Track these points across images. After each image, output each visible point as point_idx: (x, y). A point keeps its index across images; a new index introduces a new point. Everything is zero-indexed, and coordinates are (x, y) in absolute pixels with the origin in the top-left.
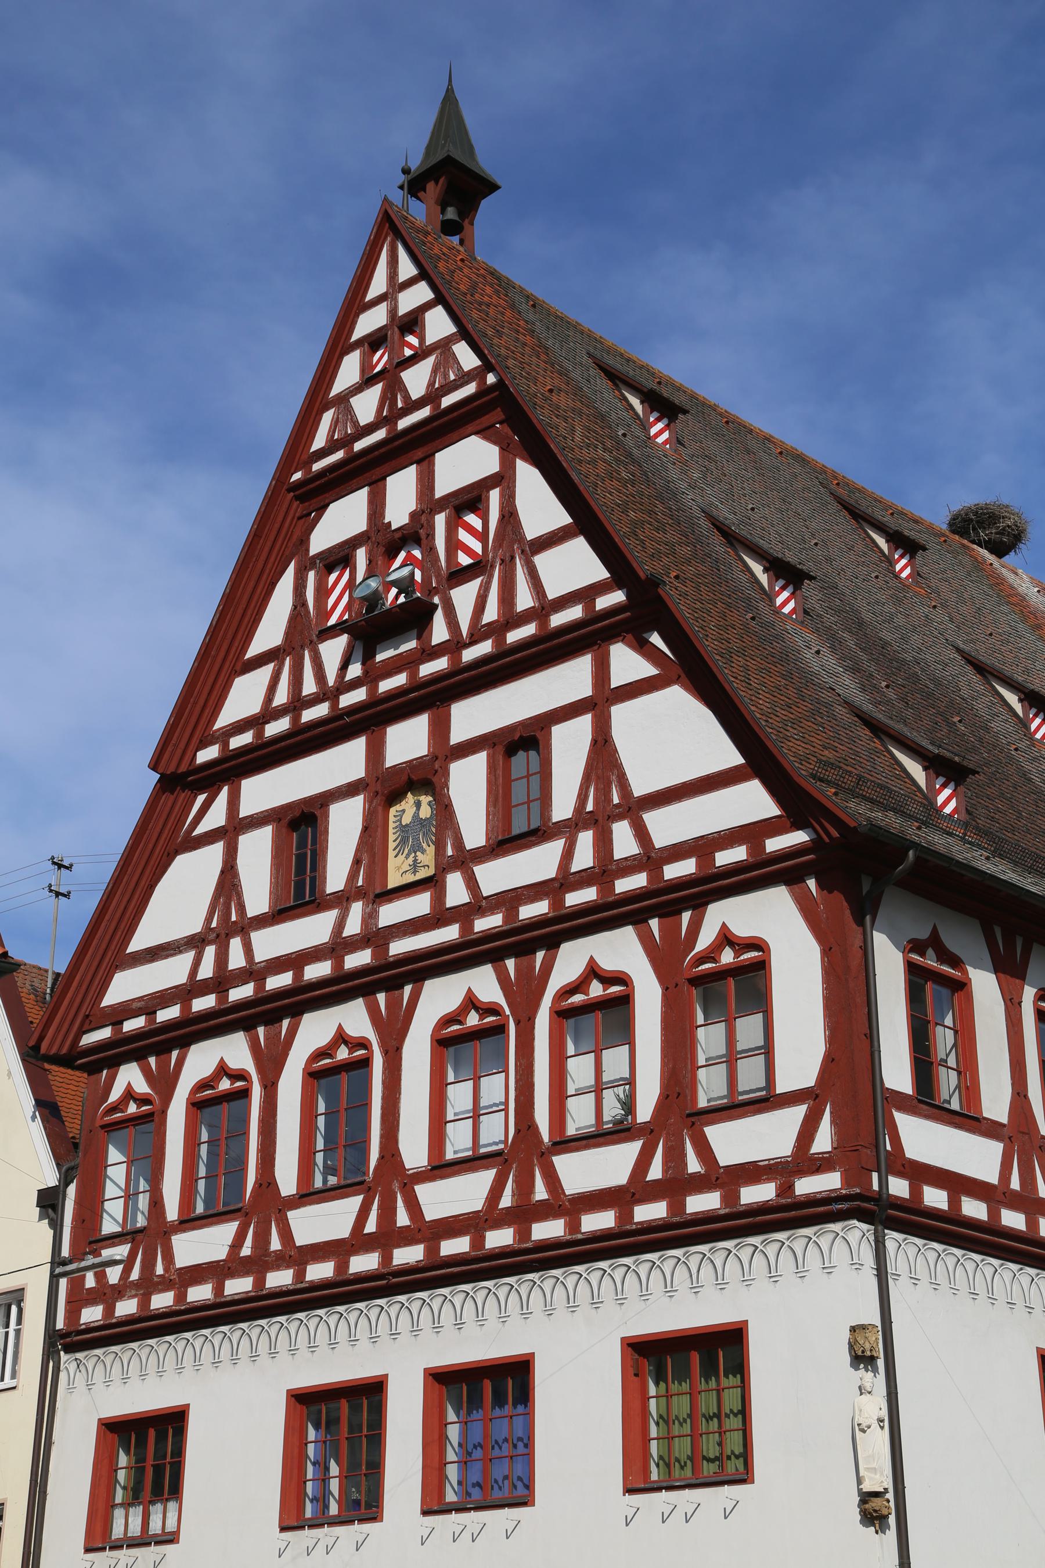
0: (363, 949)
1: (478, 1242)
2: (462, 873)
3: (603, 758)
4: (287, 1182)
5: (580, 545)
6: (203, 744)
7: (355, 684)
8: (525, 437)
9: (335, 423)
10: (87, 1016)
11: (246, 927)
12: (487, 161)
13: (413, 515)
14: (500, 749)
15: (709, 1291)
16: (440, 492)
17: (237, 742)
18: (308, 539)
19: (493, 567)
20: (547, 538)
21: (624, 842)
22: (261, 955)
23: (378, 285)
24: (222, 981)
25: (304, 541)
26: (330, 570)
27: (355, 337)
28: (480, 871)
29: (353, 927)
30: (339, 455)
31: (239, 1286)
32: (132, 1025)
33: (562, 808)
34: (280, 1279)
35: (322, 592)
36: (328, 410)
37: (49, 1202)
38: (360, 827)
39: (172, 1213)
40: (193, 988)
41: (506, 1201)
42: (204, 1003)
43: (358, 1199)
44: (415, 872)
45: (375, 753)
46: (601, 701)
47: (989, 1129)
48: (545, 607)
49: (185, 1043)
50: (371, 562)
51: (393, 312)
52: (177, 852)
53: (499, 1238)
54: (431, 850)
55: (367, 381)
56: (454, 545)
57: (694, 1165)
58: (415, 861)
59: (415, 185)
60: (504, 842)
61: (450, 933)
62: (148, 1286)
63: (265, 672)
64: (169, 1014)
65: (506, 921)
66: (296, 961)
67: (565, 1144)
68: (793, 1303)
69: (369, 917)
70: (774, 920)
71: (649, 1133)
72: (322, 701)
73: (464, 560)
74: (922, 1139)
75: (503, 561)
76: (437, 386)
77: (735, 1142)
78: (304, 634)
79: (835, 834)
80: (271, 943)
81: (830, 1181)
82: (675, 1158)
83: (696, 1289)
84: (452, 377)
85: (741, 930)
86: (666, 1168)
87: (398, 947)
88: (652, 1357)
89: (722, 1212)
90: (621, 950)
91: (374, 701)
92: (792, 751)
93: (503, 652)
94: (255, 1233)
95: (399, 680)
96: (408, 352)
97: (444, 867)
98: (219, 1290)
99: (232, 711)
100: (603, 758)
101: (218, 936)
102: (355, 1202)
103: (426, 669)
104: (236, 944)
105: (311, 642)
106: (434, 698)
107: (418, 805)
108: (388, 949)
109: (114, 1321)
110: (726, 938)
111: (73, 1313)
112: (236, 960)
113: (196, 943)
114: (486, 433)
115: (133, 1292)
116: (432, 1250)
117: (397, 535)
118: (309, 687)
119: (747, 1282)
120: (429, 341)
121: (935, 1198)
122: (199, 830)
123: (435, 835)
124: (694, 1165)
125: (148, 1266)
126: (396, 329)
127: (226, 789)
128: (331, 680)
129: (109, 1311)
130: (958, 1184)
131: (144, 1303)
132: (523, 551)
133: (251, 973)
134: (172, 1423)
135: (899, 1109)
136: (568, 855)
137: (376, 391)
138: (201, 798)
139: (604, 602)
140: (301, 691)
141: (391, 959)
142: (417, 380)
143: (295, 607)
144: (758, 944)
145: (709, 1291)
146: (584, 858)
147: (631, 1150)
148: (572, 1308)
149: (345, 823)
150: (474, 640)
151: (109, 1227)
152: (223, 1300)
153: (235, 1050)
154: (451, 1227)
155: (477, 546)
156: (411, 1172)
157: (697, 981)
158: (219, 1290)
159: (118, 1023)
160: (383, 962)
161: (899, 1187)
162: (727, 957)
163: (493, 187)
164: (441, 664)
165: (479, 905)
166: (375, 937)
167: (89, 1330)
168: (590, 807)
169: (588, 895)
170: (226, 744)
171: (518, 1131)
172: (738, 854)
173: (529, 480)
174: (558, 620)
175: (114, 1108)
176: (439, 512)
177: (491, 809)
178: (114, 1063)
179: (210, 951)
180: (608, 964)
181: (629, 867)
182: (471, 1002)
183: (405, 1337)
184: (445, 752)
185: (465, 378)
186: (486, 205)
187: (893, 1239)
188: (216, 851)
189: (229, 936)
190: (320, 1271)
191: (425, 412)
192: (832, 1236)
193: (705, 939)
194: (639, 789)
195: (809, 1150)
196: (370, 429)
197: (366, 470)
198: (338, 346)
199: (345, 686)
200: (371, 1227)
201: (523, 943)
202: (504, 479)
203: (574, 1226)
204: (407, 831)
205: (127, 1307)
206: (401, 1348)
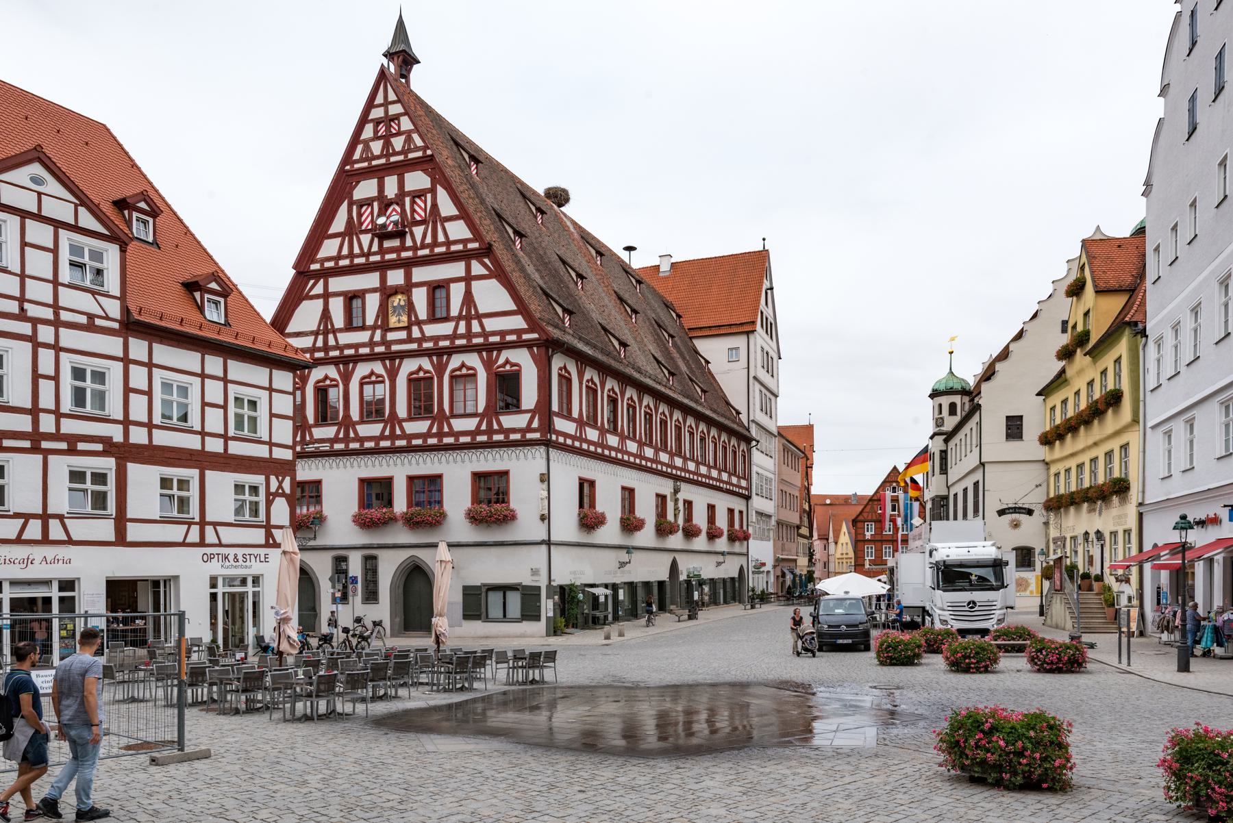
3: (468, 299)
6: (313, 262)
7: (375, 254)
11: (335, 331)
15: (498, 461)
16: (407, 189)
21: (476, 327)
23: (380, 99)
26: (362, 206)
29: (377, 338)
30: (366, 164)
33: (454, 312)
35: (360, 215)
41: (434, 430)
43: (382, 425)
45: (383, 279)
46: (468, 279)
48: (448, 243)
50: (380, 209)
53: (432, 441)
55: (376, 137)
56: (413, 211)
57: (496, 427)
60: (433, 319)
61: (414, 346)
66: (356, 346)
68: (524, 468)
69: (383, 336)
70: (523, 360)
71: (482, 416)
73: (418, 218)
74: (561, 424)
77: (508, 421)
78: (352, 230)
81: (537, 435)
82: (490, 424)
85: (512, 360)
87: (394, 348)
90: (473, 360)
91: (383, 261)
95: (394, 256)
100: (468, 299)
103: (404, 254)
104: (331, 337)
106: (408, 265)
110: (507, 362)
112: (332, 342)
113: (316, 334)
114: (425, 171)
119: (510, 459)
120: (402, 129)
121: (561, 440)
124: (496, 427)
130: (566, 435)
136: (456, 328)
138: (312, 282)
139: (470, 246)
142: (398, 143)
145: (498, 461)
147: (477, 420)
166: (384, 342)
169: (463, 342)
172: (513, 338)
173: (442, 193)
174: (453, 248)
179: (321, 338)
180: (469, 363)
181: (477, 335)
182: (420, 369)
185: (417, 149)
188: (319, 303)
193: (501, 361)
194: (481, 311)
196: (378, 157)
197: (379, 173)
198: (363, 120)
201: (440, 354)
202: (433, 191)
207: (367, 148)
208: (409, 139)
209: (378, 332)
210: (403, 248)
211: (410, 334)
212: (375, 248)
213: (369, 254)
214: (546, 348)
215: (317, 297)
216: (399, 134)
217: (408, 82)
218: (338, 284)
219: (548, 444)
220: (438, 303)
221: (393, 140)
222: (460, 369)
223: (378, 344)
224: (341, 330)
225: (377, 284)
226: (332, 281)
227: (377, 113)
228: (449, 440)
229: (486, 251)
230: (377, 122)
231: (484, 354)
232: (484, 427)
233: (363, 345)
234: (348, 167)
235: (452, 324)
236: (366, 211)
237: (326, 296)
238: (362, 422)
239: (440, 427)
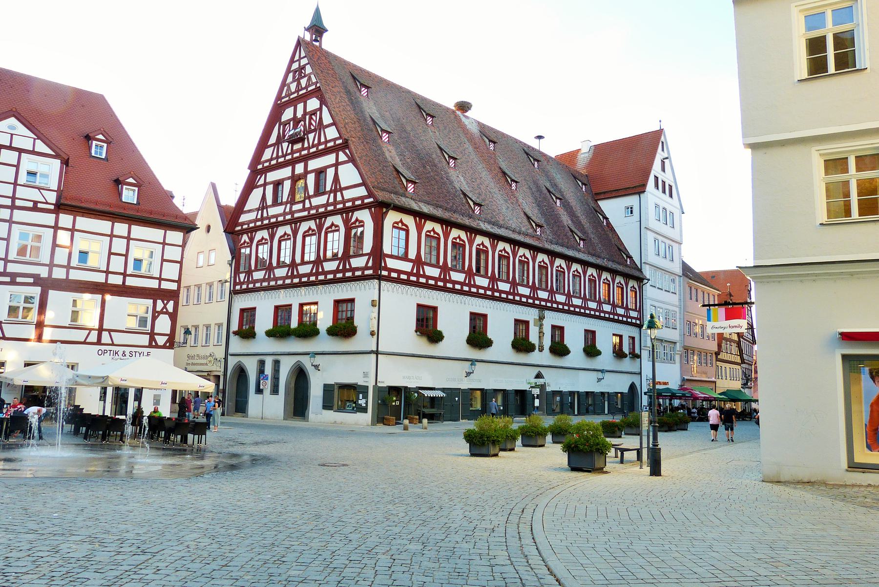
8: (323, 102)
11: (267, 207)
12: (326, 23)
17: (266, 164)
22: (270, 214)
24: (262, 219)
28: (312, 200)
29: (288, 210)
31: (265, 284)
32: (245, 227)
33: (328, 189)
34: (273, 283)
35: (284, 131)
39: (253, 268)
40: (256, 220)
42: (259, 223)
46: (337, 164)
47: (410, 261)
48: (327, 142)
49: (256, 231)
55: (294, 81)
56: (310, 124)
57: (348, 267)
59: (307, 29)
61: (306, 213)
62: (248, 282)
64: (252, 225)
66: (276, 216)
67: (326, 260)
68: (362, 294)
69: (291, 208)
73: (312, 128)
80: (273, 211)
81: (370, 272)
85: (360, 219)
87: (296, 215)
88: (337, 302)
90: (338, 220)
91: (293, 158)
93: (318, 151)
106: (305, 159)
110: (357, 220)
111: (234, 287)
112: (265, 215)
113: (258, 209)
116: (300, 280)
118: (280, 154)
121: (394, 275)
124: (348, 267)
130: (400, 272)
142: (303, 82)
144: (362, 221)
146: (331, 200)
154: (304, 275)
161: (385, 273)
162: (357, 224)
164: (305, 152)
165: (311, 208)
166: (292, 212)
169: (331, 208)
174: (329, 145)
180: (335, 223)
181: (340, 203)
182: (310, 229)
184: (306, 172)
186: (325, 35)
187: (383, 283)
190: (280, 282)
193: (353, 220)
196: (294, 93)
198: (288, 71)
201: (320, 217)
203: (326, 277)
205: (244, 287)
208: (309, 79)
209: (289, 205)
210: (303, 149)
211: (304, 205)
212: (289, 151)
213: (287, 155)
214: (380, 208)
215: (261, 186)
216: (305, 76)
217: (321, 44)
218: (272, 176)
219: (380, 278)
221: (301, 81)
222: (330, 227)
223: (287, 214)
224: (270, 206)
225: (290, 174)
229: (345, 146)
230: (295, 71)
232: (341, 268)
233: (280, 215)
235: (327, 196)
237: (265, 185)
239: (317, 269)
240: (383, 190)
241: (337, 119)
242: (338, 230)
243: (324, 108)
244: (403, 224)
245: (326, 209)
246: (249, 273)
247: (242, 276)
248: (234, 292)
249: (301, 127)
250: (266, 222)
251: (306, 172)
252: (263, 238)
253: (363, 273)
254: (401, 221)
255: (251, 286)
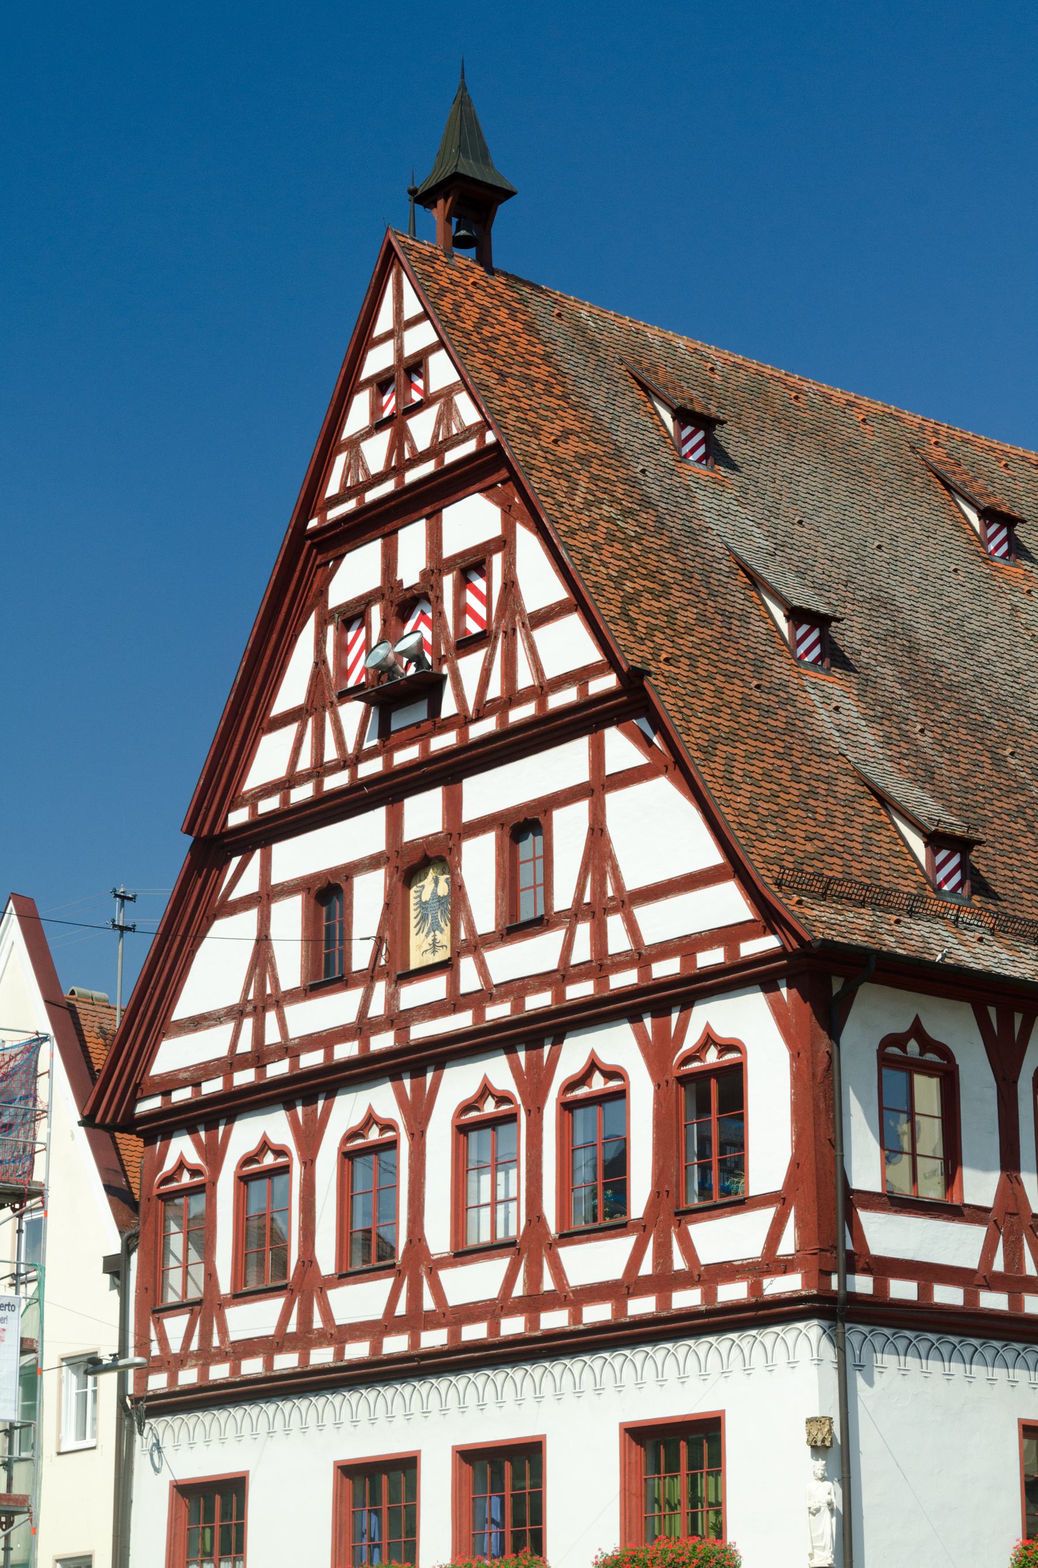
0: (387, 1030)
1: (494, 1329)
2: (474, 958)
4: (327, 1262)
5: (574, 622)
6: (234, 806)
7: (372, 754)
9: (348, 468)
10: (140, 1084)
11: (280, 1000)
13: (424, 574)
14: (507, 829)
15: (693, 1382)
16: (447, 552)
17: (269, 805)
18: (327, 590)
19: (496, 638)
20: (545, 612)
22: (296, 1031)
23: (385, 322)
24: (259, 1057)
25: (323, 593)
27: (365, 375)
28: (489, 956)
29: (377, 1008)
30: (351, 505)
31: (286, 1361)
32: (181, 1095)
33: (563, 899)
34: (322, 1356)
35: (343, 649)
36: (340, 452)
37: (115, 1267)
38: (382, 903)
39: (225, 1287)
40: (233, 1062)
41: (518, 1290)
42: (244, 1077)
43: (391, 1280)
44: (434, 952)
45: (395, 825)
46: (597, 788)
48: (543, 689)
50: (385, 621)
51: (399, 350)
52: (215, 917)
53: (513, 1326)
54: (447, 930)
55: (378, 426)
56: (462, 610)
57: (679, 1263)
58: (434, 940)
59: (426, 198)
60: (514, 928)
61: (463, 1020)
62: (206, 1357)
63: (290, 731)
64: (212, 1086)
65: (514, 1010)
69: (392, 998)
70: (750, 1025)
71: (642, 1228)
72: (343, 768)
73: (473, 628)
74: (886, 1234)
75: (505, 632)
76: (440, 439)
79: (796, 945)
81: (789, 1284)
82: (663, 1255)
83: (682, 1379)
84: (455, 431)
85: (723, 1032)
86: (655, 1265)
87: (419, 1031)
89: (703, 1308)
90: (618, 1045)
92: (755, 864)
94: (299, 1309)
96: (416, 397)
97: (457, 953)
98: (269, 1364)
99: (257, 776)
101: (255, 1008)
102: (388, 1283)
104: (271, 1017)
105: (332, 703)
106: (448, 772)
107: (436, 881)
108: (408, 1033)
109: (178, 1389)
110: (709, 1039)
111: (142, 1379)
112: (272, 1036)
113: (236, 1014)
115: (194, 1362)
116: (455, 1335)
117: (408, 595)
120: (434, 387)
121: (903, 1290)
122: (235, 895)
123: (452, 912)
124: (679, 1263)
125: (206, 1337)
126: (403, 372)
127: (258, 852)
128: (350, 748)
129: (173, 1379)
130: (927, 1273)
131: (204, 1373)
132: (523, 624)
133: (287, 1048)
134: (233, 1488)
135: (866, 1207)
137: (385, 437)
140: (322, 755)
141: (412, 1043)
143: (316, 664)
145: (693, 1382)
146: (582, 952)
148: (579, 1394)
149: (369, 894)
150: (479, 717)
151: (172, 1298)
152: (273, 1374)
153: (276, 1126)
154: (471, 1313)
155: (481, 610)
156: (435, 1257)
157: (683, 1080)
158: (269, 1364)
159: (166, 1094)
160: (405, 1044)
162: (712, 1057)
163: (509, 194)
166: (397, 1019)
167: (156, 1397)
168: (587, 899)
170: (254, 808)
171: (529, 1221)
175: (168, 1179)
176: (447, 574)
177: (500, 893)
178: (168, 1135)
179: (248, 1024)
180: (607, 1059)
181: (621, 963)
182: (486, 1090)
183: (435, 1416)
184: (458, 830)
186: (504, 211)
187: (856, 1334)
189: (265, 1009)
190: (358, 1350)
191: (428, 468)
192: (796, 1332)
193: (692, 1039)
194: (632, 882)
195: (776, 1251)
196: (379, 479)
197: (378, 522)
199: (362, 756)
200: (401, 1309)
201: (533, 1035)
202: (505, 543)
203: (576, 1317)
204: (426, 908)
205: (188, 1377)
206: (434, 1425)
207: (357, 460)
208: (448, 412)
214: (819, 981)
218: (298, 857)
220: (527, 875)
222: (584, 1078)
226: (280, 850)
227: (378, 360)
228: (555, 1320)
230: (382, 383)
231: (648, 1022)
232: (646, 1268)
233: (342, 1034)
234: (313, 523)
236: (356, 638)
237: (266, 896)
238: (344, 1276)
239: (534, 1278)
240: (826, 891)
241: (586, 582)
242: (621, 1095)
243: (527, 541)
244: (927, 1044)
245: (559, 996)
246: (206, 1309)
247: (176, 1326)
248: (139, 1410)
249: (417, 632)
250: (278, 1069)
251: (458, 830)
252: (265, 1145)
253: (756, 1288)
254: (917, 1030)
255: (219, 1372)
